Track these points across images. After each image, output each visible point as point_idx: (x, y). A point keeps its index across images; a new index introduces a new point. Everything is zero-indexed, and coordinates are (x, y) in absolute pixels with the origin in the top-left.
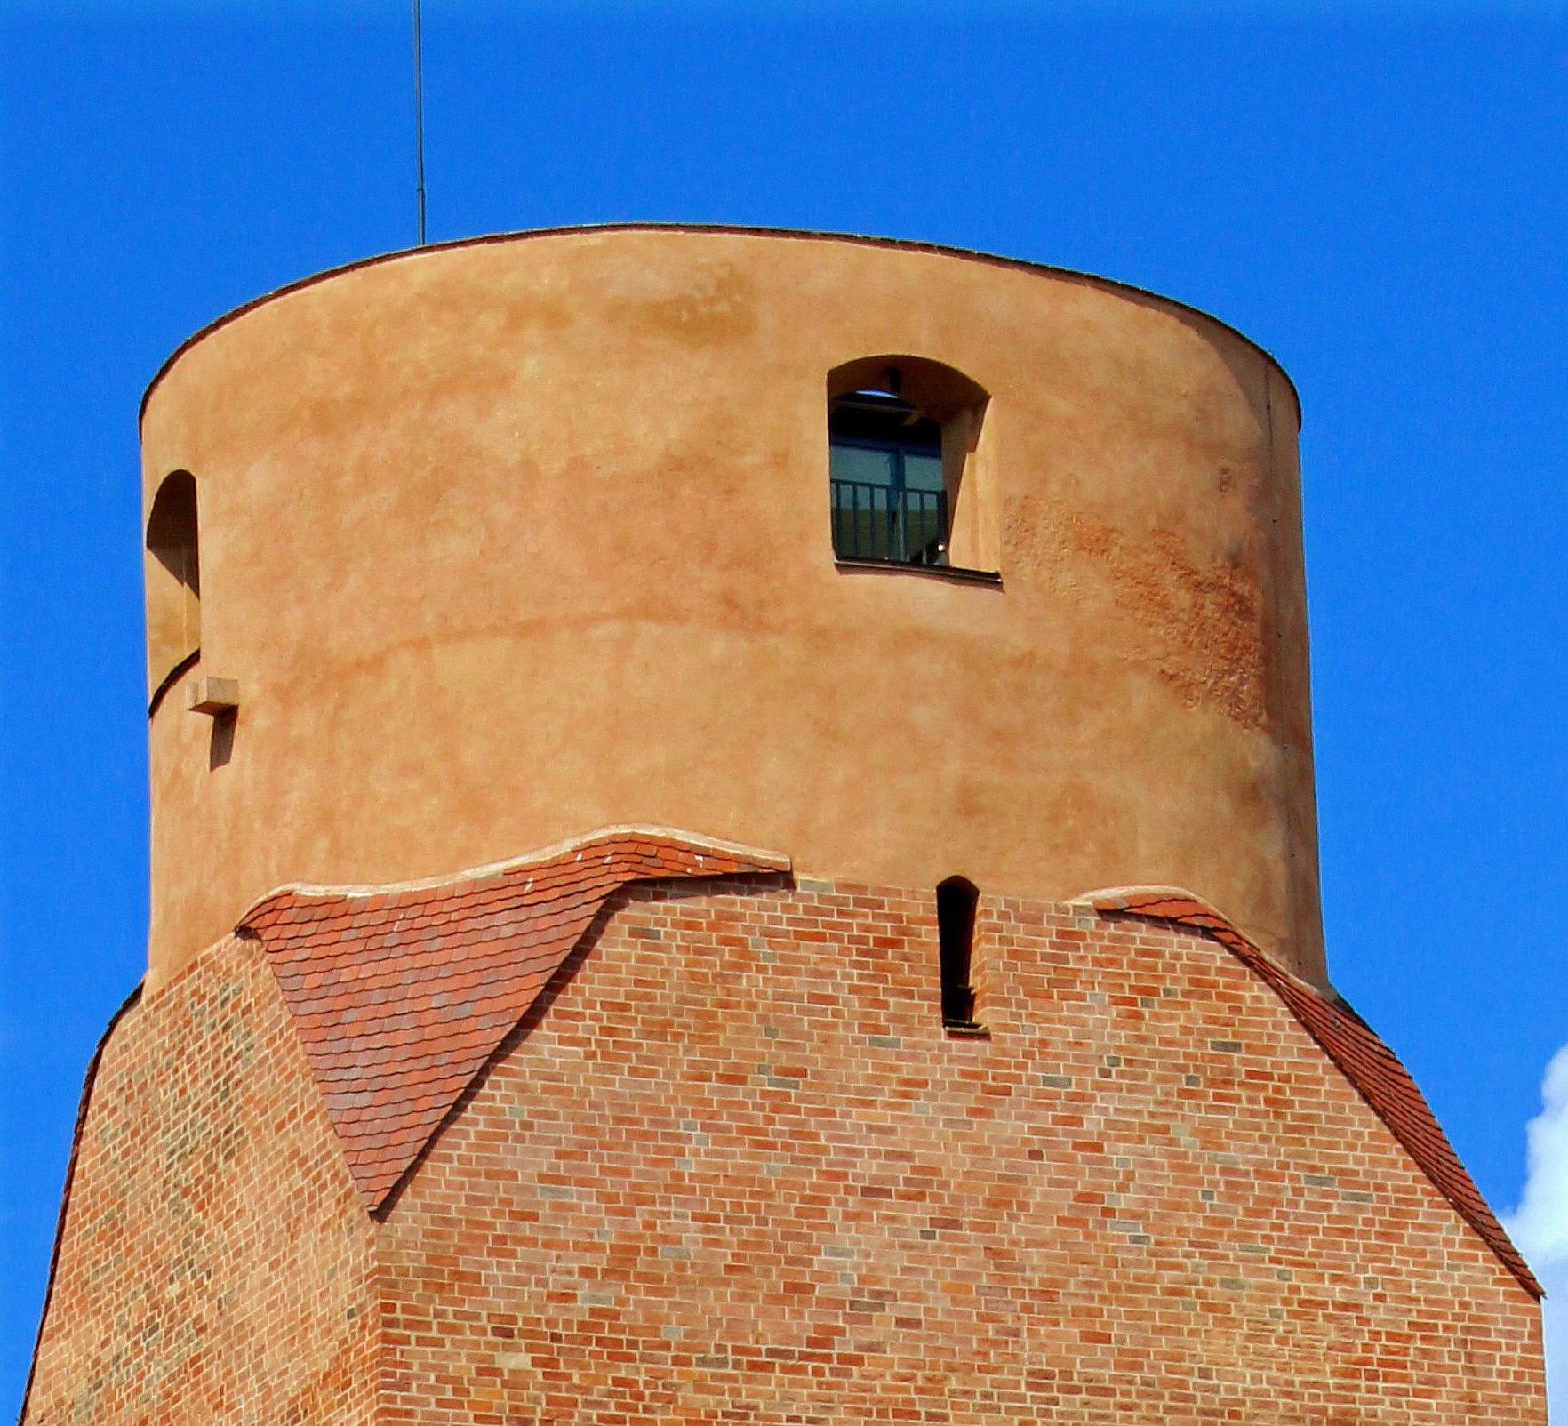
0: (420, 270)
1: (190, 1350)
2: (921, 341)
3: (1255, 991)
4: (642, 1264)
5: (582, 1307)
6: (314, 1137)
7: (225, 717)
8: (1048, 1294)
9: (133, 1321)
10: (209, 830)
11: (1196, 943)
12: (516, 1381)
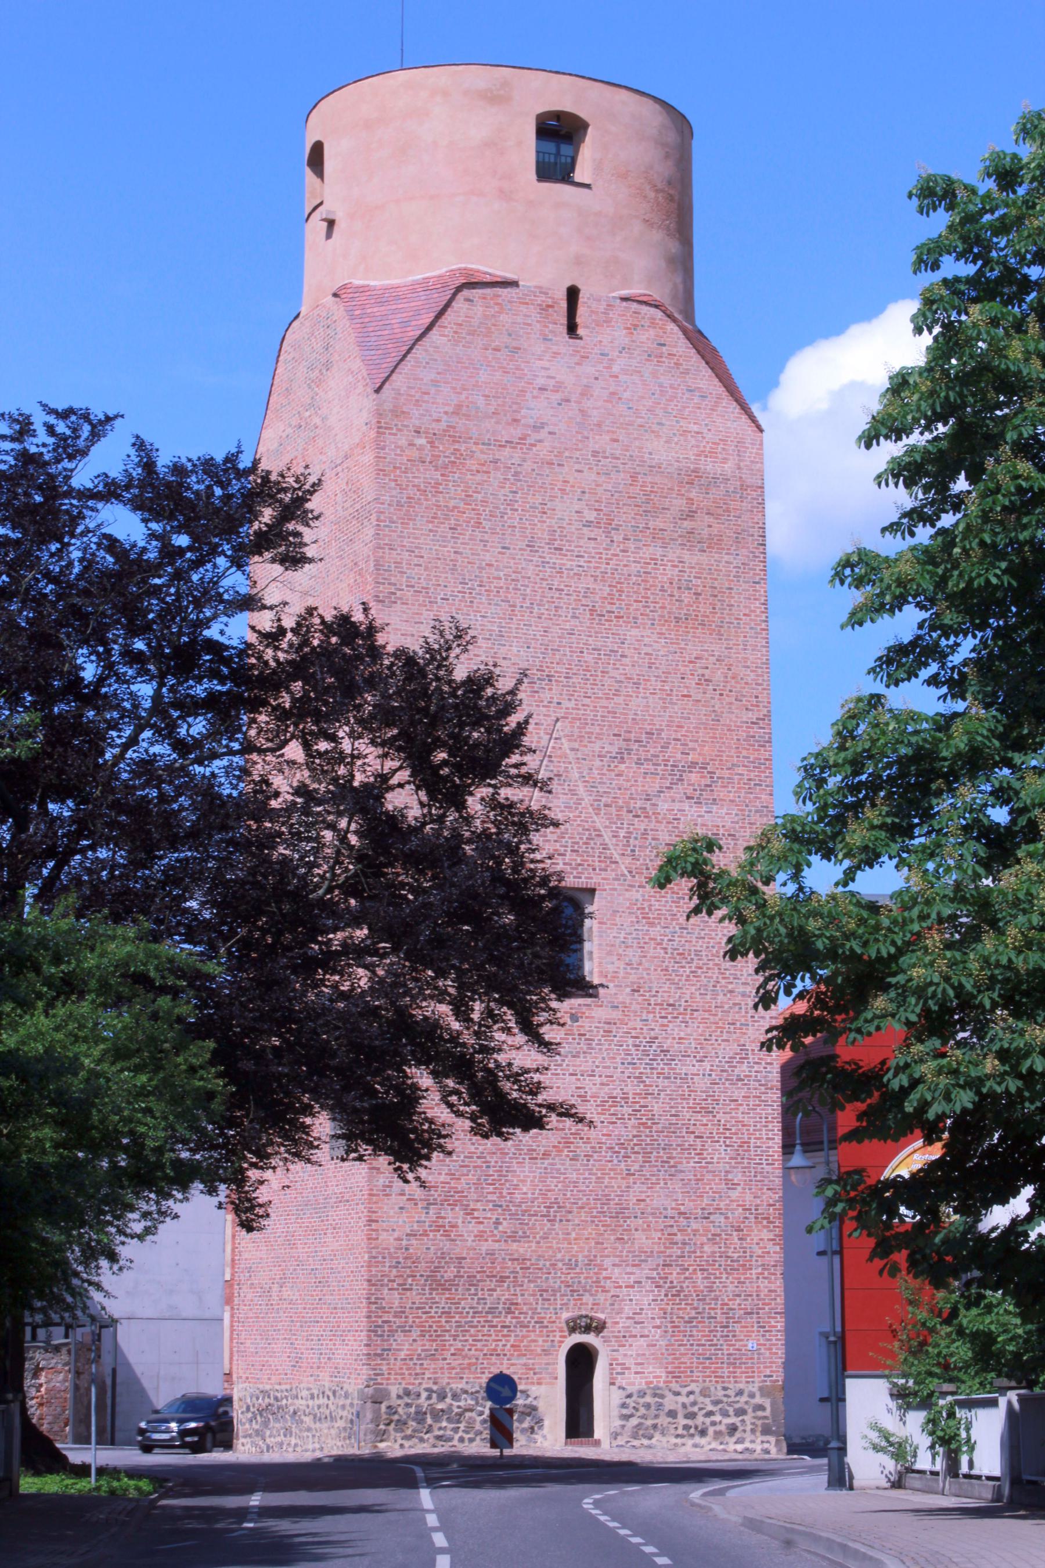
0: (402, 76)
1: (312, 434)
2: (567, 105)
3: (672, 327)
4: (464, 410)
5: (443, 425)
6: (357, 364)
7: (331, 223)
9: (294, 423)
10: (325, 265)
11: (653, 310)
12: (421, 448)
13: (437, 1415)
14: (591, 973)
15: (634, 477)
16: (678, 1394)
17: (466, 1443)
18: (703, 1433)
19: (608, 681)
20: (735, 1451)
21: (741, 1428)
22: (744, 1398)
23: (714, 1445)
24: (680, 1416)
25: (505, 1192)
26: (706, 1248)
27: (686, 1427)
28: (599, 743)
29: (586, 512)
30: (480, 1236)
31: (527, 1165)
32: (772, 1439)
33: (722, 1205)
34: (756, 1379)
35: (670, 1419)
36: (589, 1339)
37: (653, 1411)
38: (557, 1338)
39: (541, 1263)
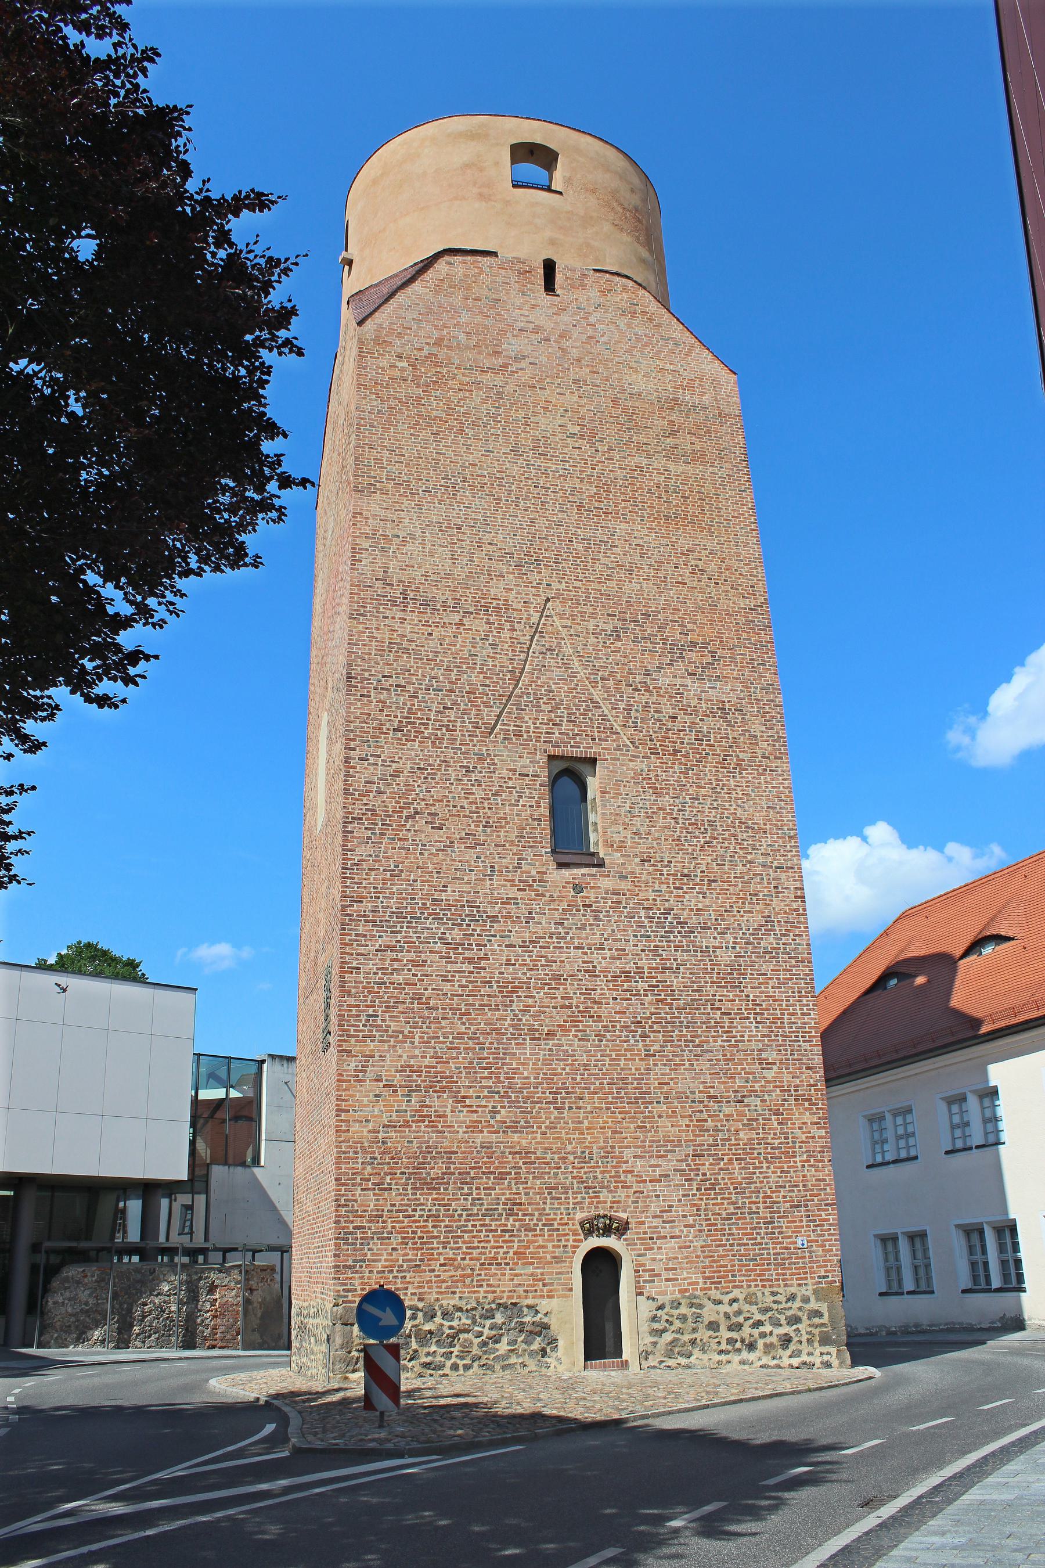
2: (538, 139)
5: (425, 352)
8: (579, 360)
11: (624, 280)
12: (403, 369)
13: (424, 1338)
14: (597, 844)
15: (615, 402)
16: (720, 1302)
17: (461, 1372)
18: (751, 1347)
19: (598, 567)
20: (791, 1366)
21: (795, 1339)
22: (797, 1303)
23: (765, 1360)
24: (723, 1328)
25: (502, 1076)
26: (742, 1135)
27: (730, 1341)
28: (593, 622)
29: (570, 426)
30: (474, 1127)
31: (528, 1046)
32: (833, 1350)
33: (757, 1087)
34: (809, 1281)
35: (711, 1333)
36: (609, 1242)
37: (690, 1324)
38: (571, 1243)
39: (549, 1156)
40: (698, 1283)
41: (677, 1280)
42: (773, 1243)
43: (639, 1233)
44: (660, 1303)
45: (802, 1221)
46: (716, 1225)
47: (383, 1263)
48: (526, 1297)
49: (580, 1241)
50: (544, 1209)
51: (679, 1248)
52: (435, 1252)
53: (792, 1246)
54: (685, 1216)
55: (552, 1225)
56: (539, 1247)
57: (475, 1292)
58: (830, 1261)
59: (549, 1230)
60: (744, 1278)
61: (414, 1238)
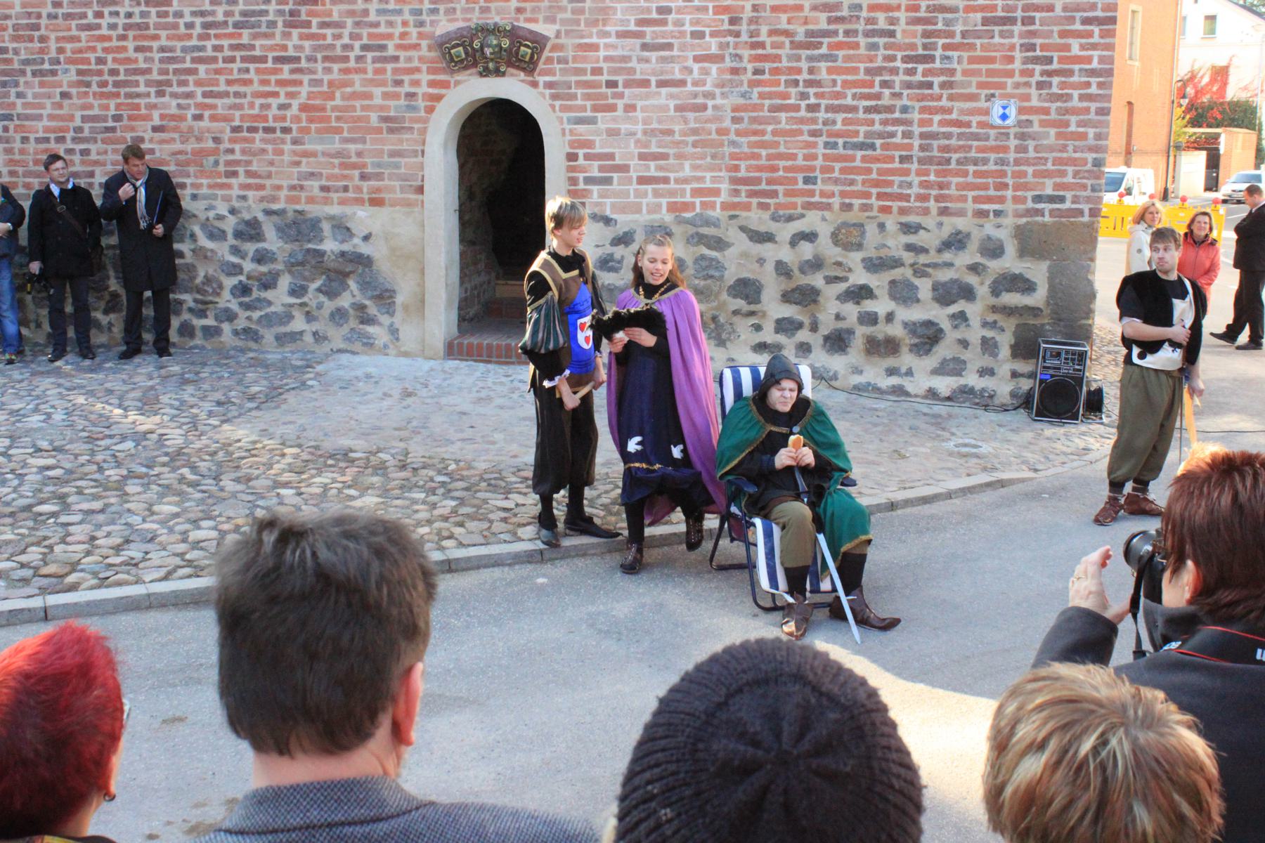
16: (767, 238)
20: (932, 394)
21: (951, 335)
22: (969, 256)
34: (1009, 206)
35: (740, 303)
38: (424, 89)
40: (717, 192)
41: (666, 180)
42: (923, 110)
43: (581, 71)
44: (620, 229)
45: (1011, 60)
46: (777, 58)
47: (45, 122)
48: (327, 201)
49: (445, 85)
50: (366, 12)
51: (679, 108)
52: (142, 101)
53: (975, 120)
54: (701, 35)
55: (383, 48)
56: (355, 96)
57: (222, 186)
58: (1074, 162)
59: (375, 60)
60: (837, 189)
61: (100, 73)
